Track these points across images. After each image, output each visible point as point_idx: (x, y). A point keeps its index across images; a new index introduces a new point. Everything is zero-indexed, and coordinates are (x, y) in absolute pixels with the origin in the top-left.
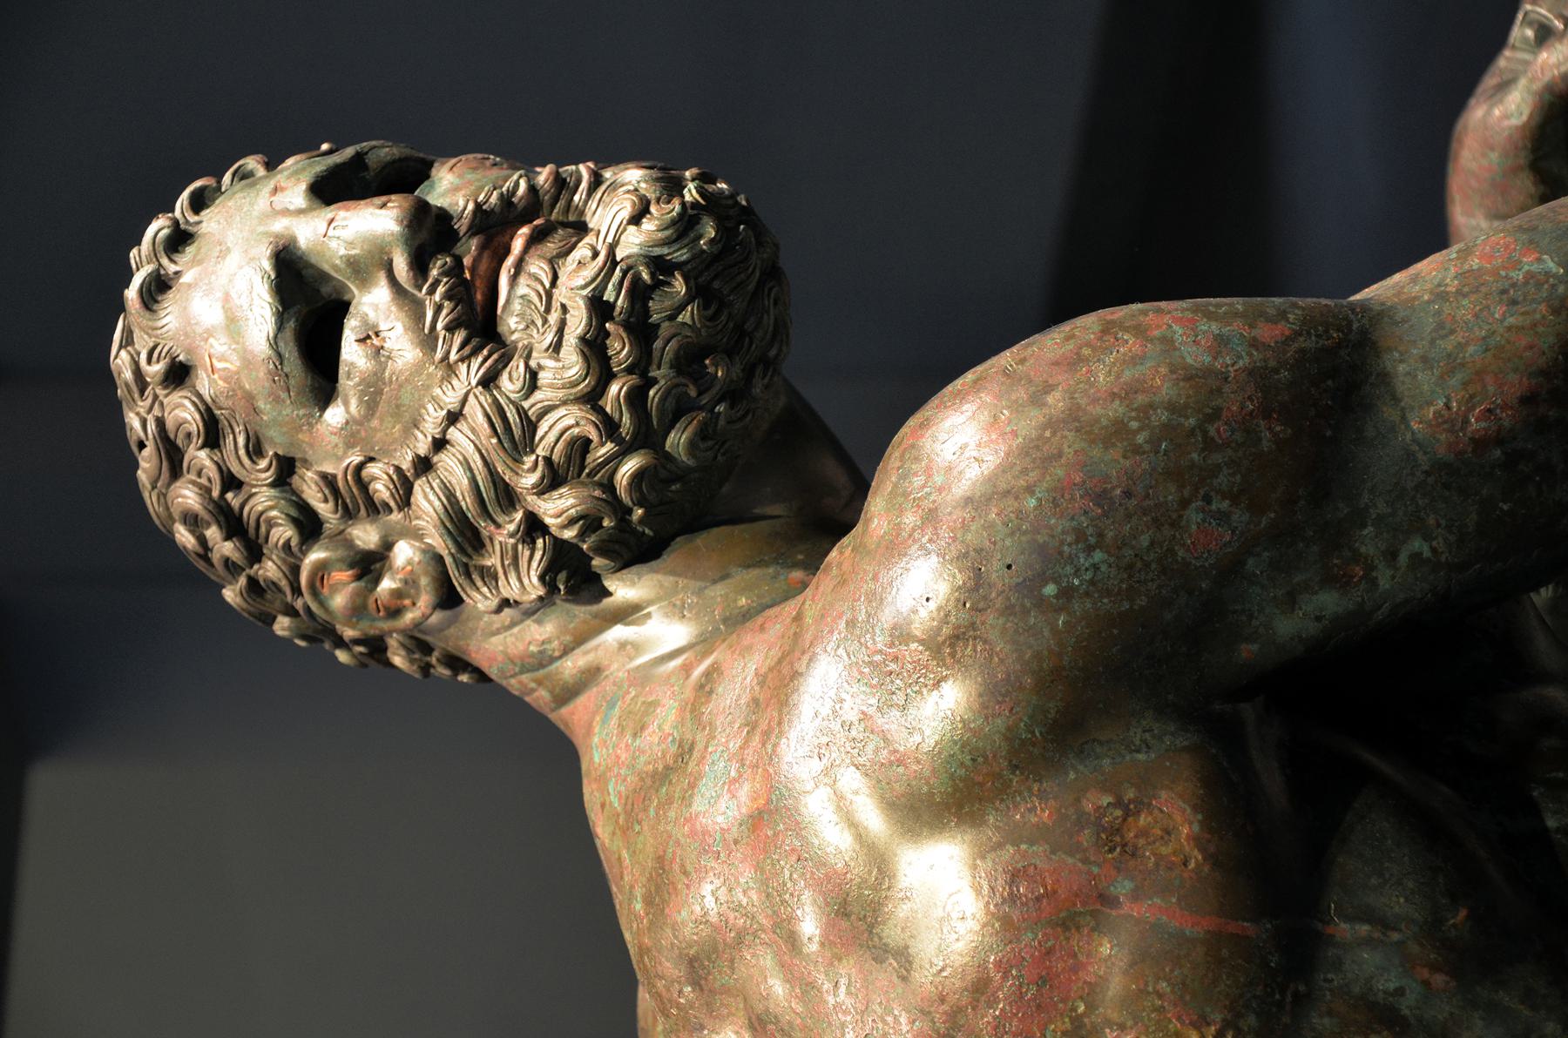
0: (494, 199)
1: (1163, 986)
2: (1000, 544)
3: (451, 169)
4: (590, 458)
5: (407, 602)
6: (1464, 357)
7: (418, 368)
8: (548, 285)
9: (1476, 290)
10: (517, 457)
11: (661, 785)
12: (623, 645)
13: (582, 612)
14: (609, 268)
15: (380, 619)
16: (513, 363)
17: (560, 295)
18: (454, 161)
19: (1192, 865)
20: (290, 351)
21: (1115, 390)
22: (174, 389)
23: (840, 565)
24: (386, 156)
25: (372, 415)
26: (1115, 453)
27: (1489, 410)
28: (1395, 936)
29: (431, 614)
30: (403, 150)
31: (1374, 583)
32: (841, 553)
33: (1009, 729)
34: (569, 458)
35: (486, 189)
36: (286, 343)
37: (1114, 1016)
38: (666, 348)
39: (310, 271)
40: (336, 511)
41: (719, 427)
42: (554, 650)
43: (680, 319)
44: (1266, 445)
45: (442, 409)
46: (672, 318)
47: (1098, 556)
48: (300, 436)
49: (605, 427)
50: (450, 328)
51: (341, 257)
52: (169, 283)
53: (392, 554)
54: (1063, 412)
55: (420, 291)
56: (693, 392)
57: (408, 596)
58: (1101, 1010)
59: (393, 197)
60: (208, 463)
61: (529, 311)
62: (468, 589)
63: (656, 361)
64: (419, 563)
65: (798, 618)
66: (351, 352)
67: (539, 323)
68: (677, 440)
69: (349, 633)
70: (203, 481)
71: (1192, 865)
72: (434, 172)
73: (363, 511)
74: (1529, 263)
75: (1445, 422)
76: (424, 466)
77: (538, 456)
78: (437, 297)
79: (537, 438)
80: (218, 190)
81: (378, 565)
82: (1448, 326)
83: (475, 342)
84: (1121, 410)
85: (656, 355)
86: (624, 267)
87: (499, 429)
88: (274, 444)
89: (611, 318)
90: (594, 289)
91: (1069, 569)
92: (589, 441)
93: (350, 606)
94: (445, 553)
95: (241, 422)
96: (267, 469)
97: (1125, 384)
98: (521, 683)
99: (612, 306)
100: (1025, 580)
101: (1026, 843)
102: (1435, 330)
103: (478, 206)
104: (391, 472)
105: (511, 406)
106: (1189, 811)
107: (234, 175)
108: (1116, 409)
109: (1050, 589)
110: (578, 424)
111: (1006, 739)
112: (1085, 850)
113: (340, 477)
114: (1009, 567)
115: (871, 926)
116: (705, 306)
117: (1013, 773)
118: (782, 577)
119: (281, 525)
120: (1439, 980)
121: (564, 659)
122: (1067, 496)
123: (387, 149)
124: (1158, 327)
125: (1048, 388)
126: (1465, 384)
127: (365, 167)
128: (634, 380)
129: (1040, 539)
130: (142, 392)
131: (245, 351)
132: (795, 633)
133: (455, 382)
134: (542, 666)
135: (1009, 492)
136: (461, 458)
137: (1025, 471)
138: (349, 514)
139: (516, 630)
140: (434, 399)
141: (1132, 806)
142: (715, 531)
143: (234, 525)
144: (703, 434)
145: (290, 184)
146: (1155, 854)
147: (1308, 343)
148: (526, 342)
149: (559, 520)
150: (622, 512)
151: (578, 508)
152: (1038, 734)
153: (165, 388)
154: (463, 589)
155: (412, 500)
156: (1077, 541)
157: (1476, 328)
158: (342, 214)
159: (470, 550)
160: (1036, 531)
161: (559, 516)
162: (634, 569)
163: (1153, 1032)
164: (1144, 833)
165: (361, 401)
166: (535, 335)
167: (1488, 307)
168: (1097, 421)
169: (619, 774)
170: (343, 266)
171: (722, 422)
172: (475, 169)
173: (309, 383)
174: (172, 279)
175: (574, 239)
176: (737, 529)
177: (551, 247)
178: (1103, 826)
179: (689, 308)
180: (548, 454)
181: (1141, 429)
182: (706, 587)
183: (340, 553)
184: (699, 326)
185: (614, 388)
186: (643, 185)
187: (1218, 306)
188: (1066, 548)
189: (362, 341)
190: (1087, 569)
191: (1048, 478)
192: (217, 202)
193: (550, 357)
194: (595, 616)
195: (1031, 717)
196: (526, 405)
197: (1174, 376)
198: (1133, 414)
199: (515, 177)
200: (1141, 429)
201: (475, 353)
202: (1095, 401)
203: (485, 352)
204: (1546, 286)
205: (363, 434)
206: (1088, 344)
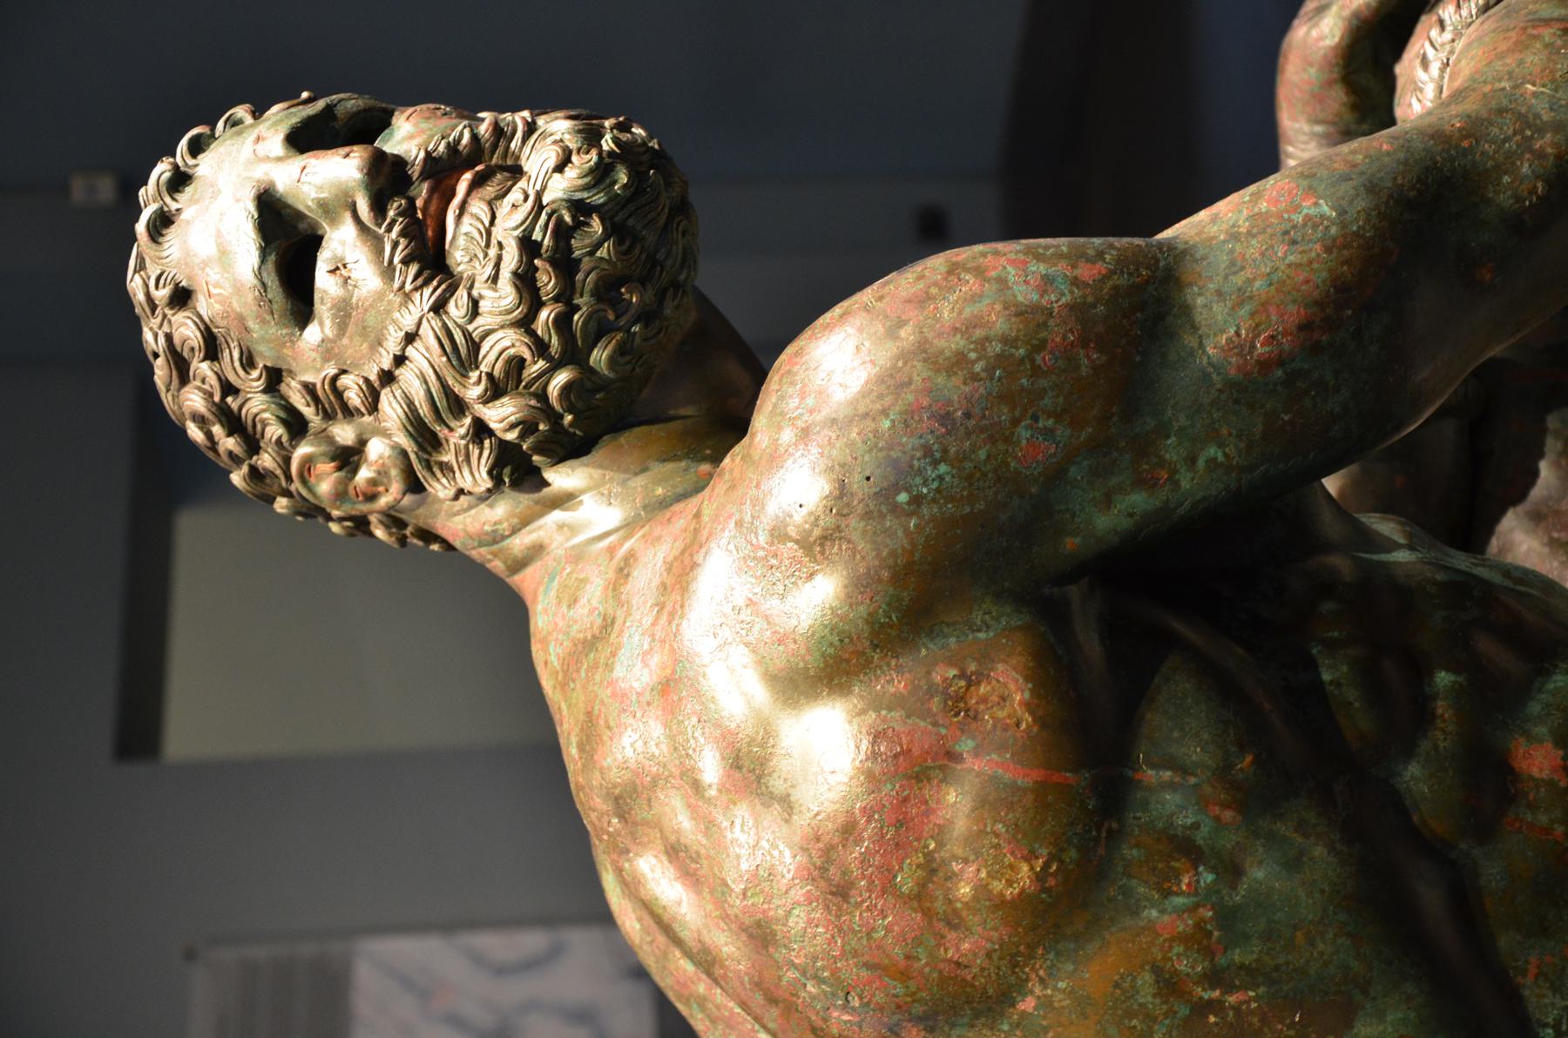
0: (441, 148)
1: (999, 827)
2: (860, 458)
3: (408, 118)
4: (525, 373)
5: (381, 489)
6: (1252, 291)
7: (380, 296)
8: (487, 224)
9: (1264, 231)
10: (464, 372)
11: (590, 651)
12: (561, 526)
13: (525, 500)
14: (536, 212)
15: (360, 502)
16: (458, 293)
17: (498, 234)
18: (411, 110)
19: (1024, 726)
20: (272, 280)
21: (957, 325)
22: (179, 310)
23: (731, 471)
25: (343, 335)
26: (956, 381)
27: (1272, 337)
28: (1193, 780)
29: (402, 499)
30: (367, 101)
31: (1177, 484)
32: (733, 460)
33: (870, 614)
34: (507, 373)
35: (436, 138)
36: (268, 274)
37: (959, 852)
38: (587, 279)
39: (288, 210)
40: (318, 414)
41: (635, 344)
42: (504, 530)
43: (598, 254)
44: (1084, 371)
45: (401, 330)
46: (592, 253)
47: (943, 468)
48: (285, 351)
49: (537, 348)
50: (406, 262)
51: (313, 200)
52: (173, 218)
53: (366, 449)
54: (913, 345)
55: (380, 228)
56: (611, 316)
57: (382, 484)
58: (948, 847)
59: (355, 148)
60: (209, 373)
61: (472, 247)
62: (430, 480)
63: (579, 290)
64: (389, 457)
65: (698, 516)
66: (324, 282)
67: (481, 256)
68: (600, 357)
69: (336, 513)
70: (206, 387)
71: (1024, 726)
72: (394, 120)
73: (340, 415)
74: (1308, 208)
75: (1235, 347)
76: (388, 378)
77: (481, 372)
78: (394, 235)
79: (480, 357)
80: (213, 137)
81: (356, 458)
82: (1239, 263)
83: (426, 273)
84: (962, 343)
85: (579, 285)
86: (549, 211)
87: (448, 349)
88: (265, 357)
89: (539, 255)
90: (524, 231)
91: (918, 480)
92: (523, 360)
93: (333, 492)
94: (409, 450)
95: (235, 338)
96: (259, 379)
97: (966, 319)
98: (480, 554)
99: (539, 245)
100: (881, 490)
101: (885, 709)
102: (1228, 267)
103: (428, 154)
106: (1021, 680)
107: (226, 123)
108: (958, 342)
109: (903, 497)
110: (513, 345)
111: (867, 622)
112: (935, 715)
113: (319, 386)
114: (868, 479)
115: (759, 777)
116: (619, 243)
117: (874, 651)
118: (692, 470)
119: (272, 425)
120: (1228, 815)
121: (513, 537)
122: (916, 418)
123: (353, 101)
124: (995, 268)
125: (901, 324)
126: (1252, 315)
127: (334, 118)
128: (559, 307)
129: (894, 454)
130: (153, 312)
131: (235, 280)
132: (695, 529)
133: (411, 306)
134: (495, 542)
135: (867, 414)
136: (418, 373)
137: (881, 397)
138: (328, 416)
139: (473, 512)
140: (394, 322)
141: (974, 678)
142: (637, 431)
143: (234, 423)
144: (621, 351)
145: (270, 135)
146: (993, 718)
147: (1121, 281)
148: (470, 273)
149: (502, 425)
150: (555, 418)
151: (517, 416)
152: (894, 618)
153: (172, 309)
154: (426, 480)
155: (380, 406)
156: (925, 457)
157: (1262, 265)
158: (313, 161)
159: (429, 449)
160: (890, 448)
161: (502, 421)
162: (569, 463)
163: (992, 864)
164: (984, 700)
165: (333, 323)
167: (1272, 246)
168: (942, 352)
169: (557, 639)
170: (314, 207)
171: (638, 340)
172: (428, 118)
173: (289, 307)
174: (174, 215)
175: (510, 183)
176: (654, 428)
177: (490, 190)
178: (949, 695)
179: (606, 245)
180: (489, 370)
181: (978, 359)
182: (628, 479)
183: (323, 448)
184: (614, 260)
185: (544, 314)
186: (567, 137)
187: (1047, 248)
188: (915, 462)
189: (333, 272)
190: (933, 480)
191: (900, 402)
192: (212, 147)
193: (489, 288)
194: (537, 503)
195: (889, 604)
196: (470, 328)
197: (1007, 312)
198: (972, 346)
199: (460, 127)
200: (978, 359)
201: (426, 283)
202: (940, 335)
203: (435, 283)
204: (1321, 228)
205: (336, 350)
206: (936, 284)
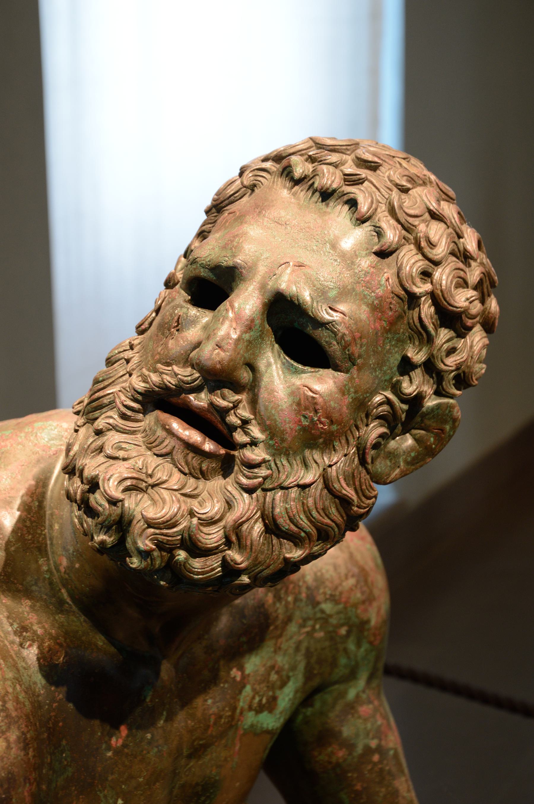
8: (155, 450)
24: (327, 342)
36: (195, 269)
83: (140, 398)
104: (143, 327)
105: (99, 414)
118: (64, 553)
123: (335, 343)
136: (111, 375)
166: (143, 435)
177: (179, 456)
